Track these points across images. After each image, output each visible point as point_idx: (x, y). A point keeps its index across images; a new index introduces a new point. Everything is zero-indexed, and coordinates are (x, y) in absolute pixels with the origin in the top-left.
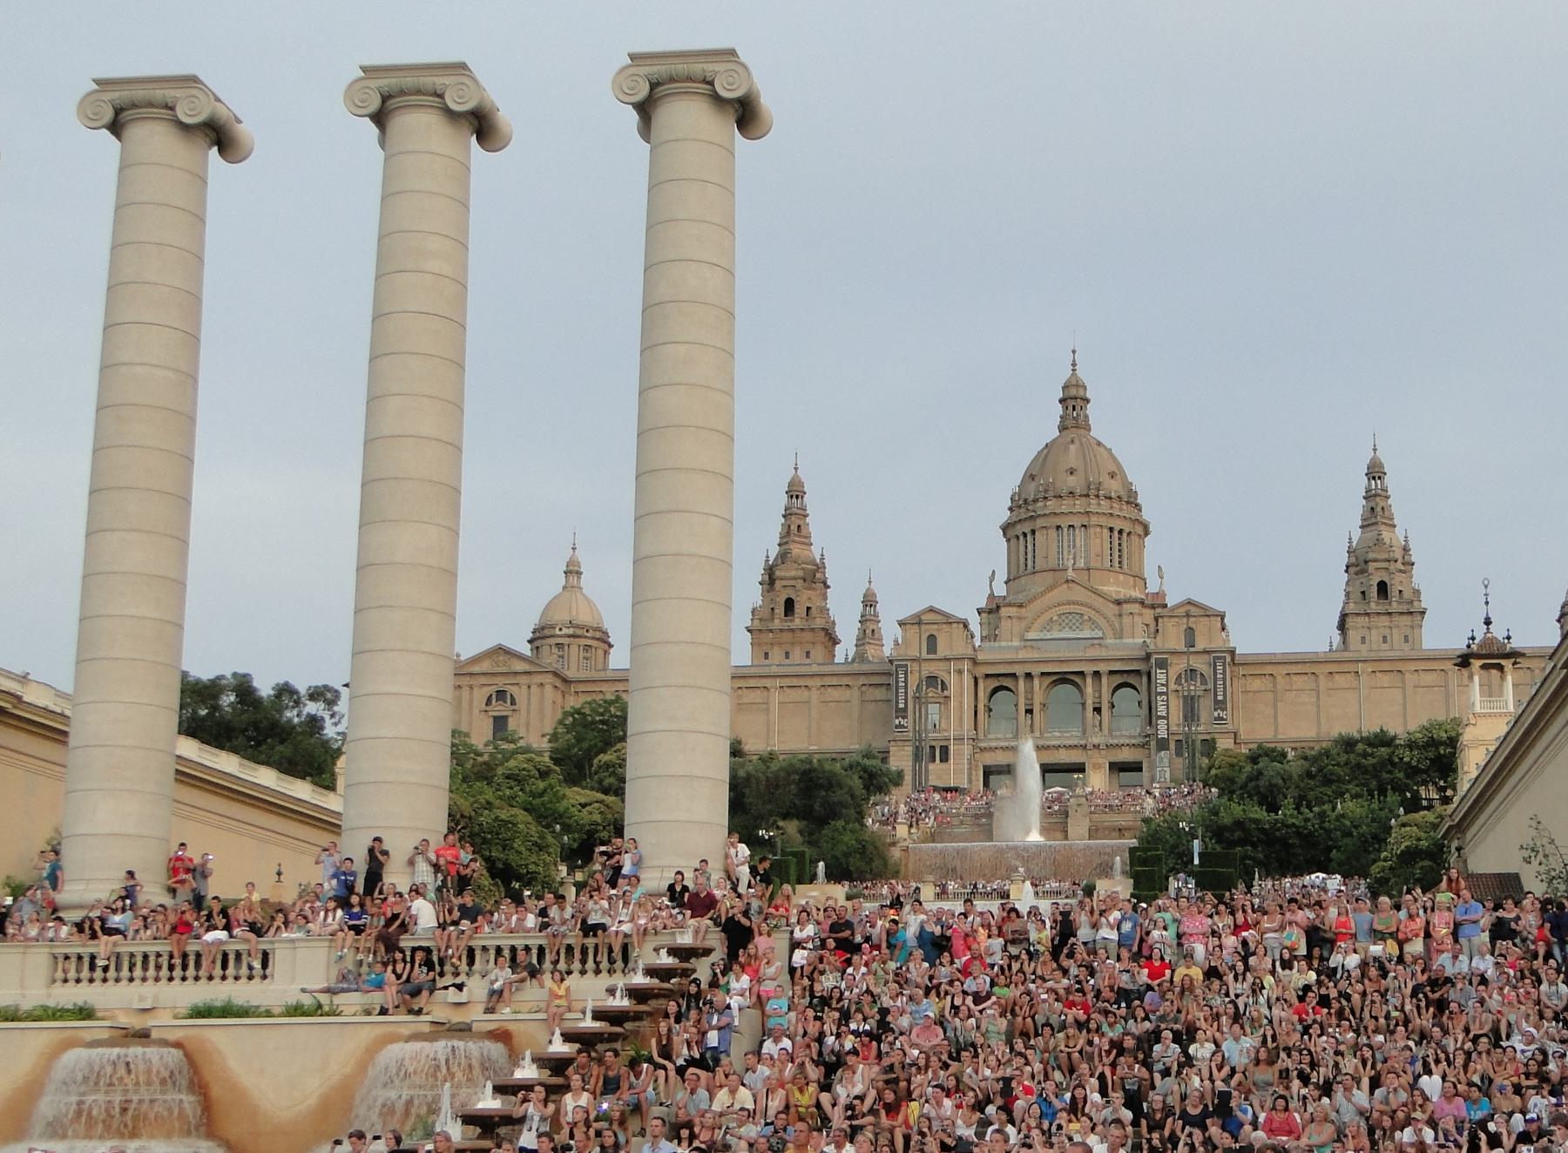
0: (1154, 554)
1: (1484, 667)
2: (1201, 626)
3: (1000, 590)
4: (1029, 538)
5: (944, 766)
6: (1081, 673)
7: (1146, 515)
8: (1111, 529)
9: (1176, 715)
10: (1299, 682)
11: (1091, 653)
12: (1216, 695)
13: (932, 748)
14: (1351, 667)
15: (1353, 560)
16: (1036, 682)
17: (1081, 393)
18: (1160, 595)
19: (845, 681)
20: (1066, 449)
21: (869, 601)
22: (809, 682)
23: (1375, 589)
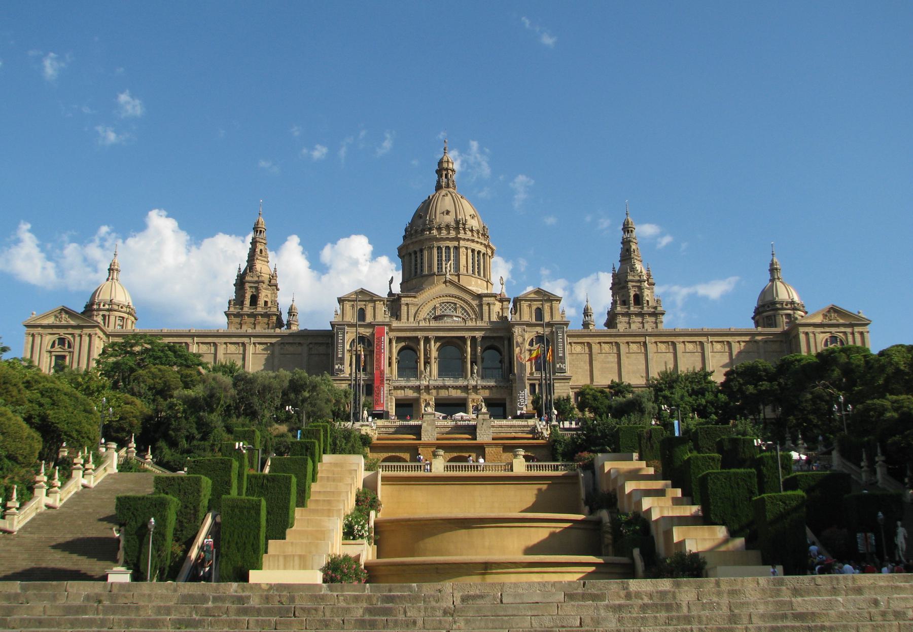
2: (547, 306)
4: (418, 255)
6: (463, 339)
8: (473, 251)
11: (470, 324)
12: (558, 353)
14: (642, 339)
15: (617, 281)
16: (433, 342)
17: (451, 166)
19: (298, 340)
23: (632, 298)
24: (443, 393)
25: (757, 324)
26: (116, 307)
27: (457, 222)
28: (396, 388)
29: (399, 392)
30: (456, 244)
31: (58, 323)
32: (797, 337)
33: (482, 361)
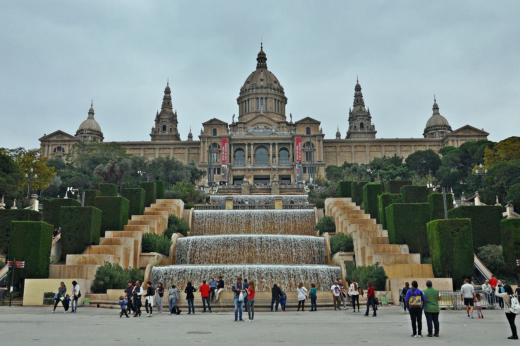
3: (236, 120)
6: (268, 144)
9: (304, 159)
10: (345, 149)
13: (215, 169)
16: (252, 147)
18: (291, 122)
20: (259, 73)
22: (170, 147)
25: (425, 137)
26: (92, 132)
28: (233, 170)
29: (235, 172)
31: (58, 139)
33: (279, 156)
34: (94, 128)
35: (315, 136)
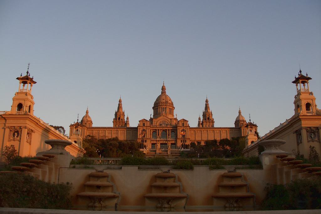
0: (175, 112)
1: (250, 127)
3: (152, 117)
5: (146, 143)
6: (166, 130)
7: (174, 106)
8: (170, 108)
19: (130, 130)
21: (127, 118)
24: (162, 142)
27: (166, 102)
30: (166, 107)
32: (241, 130)
34: (89, 119)
35: (186, 127)
